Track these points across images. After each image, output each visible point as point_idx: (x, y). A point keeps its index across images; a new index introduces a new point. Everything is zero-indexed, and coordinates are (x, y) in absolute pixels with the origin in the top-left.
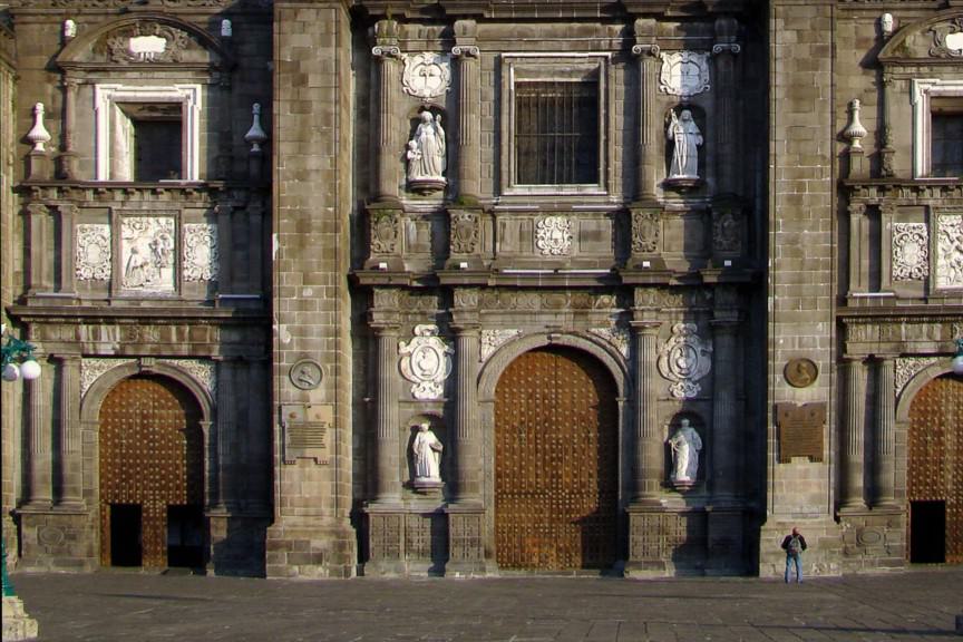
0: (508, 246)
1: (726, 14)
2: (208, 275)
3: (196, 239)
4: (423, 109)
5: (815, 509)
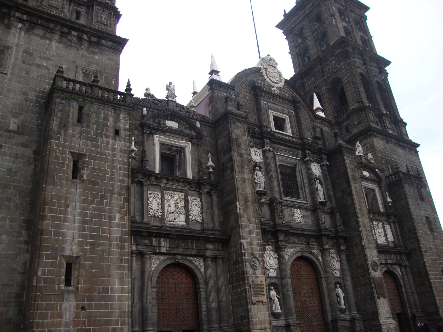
0: (287, 217)
1: (325, 154)
2: (200, 219)
3: (193, 203)
4: (256, 166)
5: (388, 316)
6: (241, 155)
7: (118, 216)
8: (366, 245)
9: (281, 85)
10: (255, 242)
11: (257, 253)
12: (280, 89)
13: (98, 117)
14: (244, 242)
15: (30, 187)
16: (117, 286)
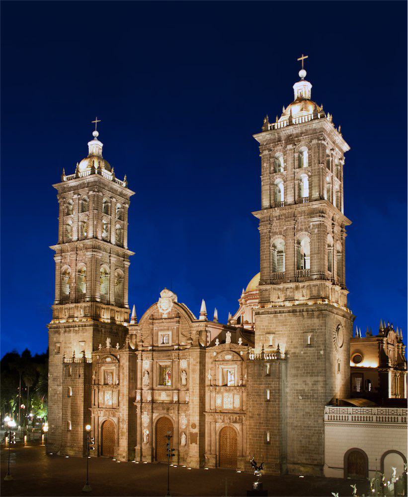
6: (123, 374)
8: (191, 414)
9: (170, 310)
10: (125, 414)
12: (169, 313)
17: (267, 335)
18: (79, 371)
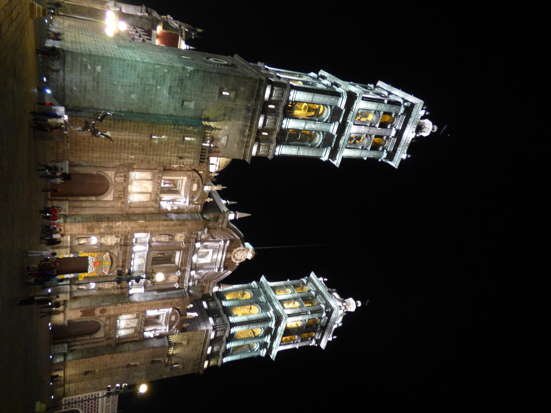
7: (133, 157)
8: (117, 307)
9: (233, 260)
10: (120, 230)
11: (114, 230)
12: (230, 259)
13: (189, 148)
14: (120, 223)
15: (151, 112)
16: (95, 155)
17: (187, 341)
18: (188, 157)
